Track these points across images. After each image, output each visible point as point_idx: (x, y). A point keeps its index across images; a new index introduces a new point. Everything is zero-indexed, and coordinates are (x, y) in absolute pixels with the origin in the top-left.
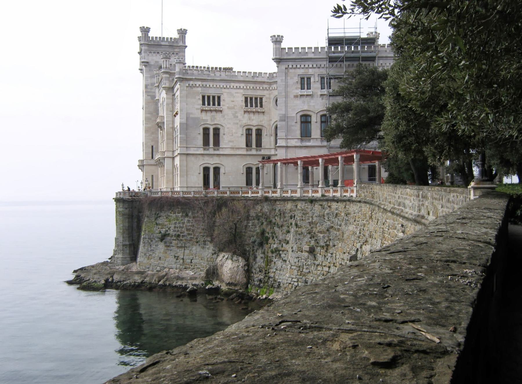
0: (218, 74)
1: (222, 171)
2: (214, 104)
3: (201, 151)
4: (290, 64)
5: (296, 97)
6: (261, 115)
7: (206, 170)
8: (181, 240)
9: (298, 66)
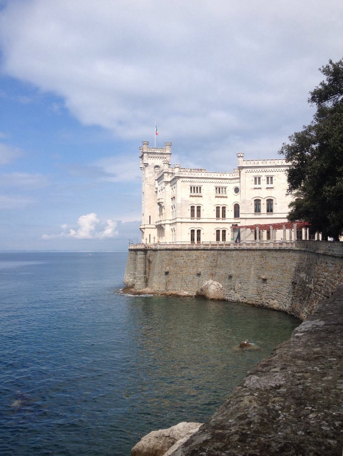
0: (200, 174)
1: (202, 232)
2: (197, 192)
3: (190, 220)
4: (248, 170)
5: (252, 189)
6: (225, 199)
7: (193, 231)
8: (180, 273)
9: (253, 171)
